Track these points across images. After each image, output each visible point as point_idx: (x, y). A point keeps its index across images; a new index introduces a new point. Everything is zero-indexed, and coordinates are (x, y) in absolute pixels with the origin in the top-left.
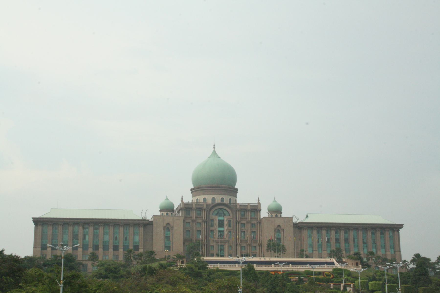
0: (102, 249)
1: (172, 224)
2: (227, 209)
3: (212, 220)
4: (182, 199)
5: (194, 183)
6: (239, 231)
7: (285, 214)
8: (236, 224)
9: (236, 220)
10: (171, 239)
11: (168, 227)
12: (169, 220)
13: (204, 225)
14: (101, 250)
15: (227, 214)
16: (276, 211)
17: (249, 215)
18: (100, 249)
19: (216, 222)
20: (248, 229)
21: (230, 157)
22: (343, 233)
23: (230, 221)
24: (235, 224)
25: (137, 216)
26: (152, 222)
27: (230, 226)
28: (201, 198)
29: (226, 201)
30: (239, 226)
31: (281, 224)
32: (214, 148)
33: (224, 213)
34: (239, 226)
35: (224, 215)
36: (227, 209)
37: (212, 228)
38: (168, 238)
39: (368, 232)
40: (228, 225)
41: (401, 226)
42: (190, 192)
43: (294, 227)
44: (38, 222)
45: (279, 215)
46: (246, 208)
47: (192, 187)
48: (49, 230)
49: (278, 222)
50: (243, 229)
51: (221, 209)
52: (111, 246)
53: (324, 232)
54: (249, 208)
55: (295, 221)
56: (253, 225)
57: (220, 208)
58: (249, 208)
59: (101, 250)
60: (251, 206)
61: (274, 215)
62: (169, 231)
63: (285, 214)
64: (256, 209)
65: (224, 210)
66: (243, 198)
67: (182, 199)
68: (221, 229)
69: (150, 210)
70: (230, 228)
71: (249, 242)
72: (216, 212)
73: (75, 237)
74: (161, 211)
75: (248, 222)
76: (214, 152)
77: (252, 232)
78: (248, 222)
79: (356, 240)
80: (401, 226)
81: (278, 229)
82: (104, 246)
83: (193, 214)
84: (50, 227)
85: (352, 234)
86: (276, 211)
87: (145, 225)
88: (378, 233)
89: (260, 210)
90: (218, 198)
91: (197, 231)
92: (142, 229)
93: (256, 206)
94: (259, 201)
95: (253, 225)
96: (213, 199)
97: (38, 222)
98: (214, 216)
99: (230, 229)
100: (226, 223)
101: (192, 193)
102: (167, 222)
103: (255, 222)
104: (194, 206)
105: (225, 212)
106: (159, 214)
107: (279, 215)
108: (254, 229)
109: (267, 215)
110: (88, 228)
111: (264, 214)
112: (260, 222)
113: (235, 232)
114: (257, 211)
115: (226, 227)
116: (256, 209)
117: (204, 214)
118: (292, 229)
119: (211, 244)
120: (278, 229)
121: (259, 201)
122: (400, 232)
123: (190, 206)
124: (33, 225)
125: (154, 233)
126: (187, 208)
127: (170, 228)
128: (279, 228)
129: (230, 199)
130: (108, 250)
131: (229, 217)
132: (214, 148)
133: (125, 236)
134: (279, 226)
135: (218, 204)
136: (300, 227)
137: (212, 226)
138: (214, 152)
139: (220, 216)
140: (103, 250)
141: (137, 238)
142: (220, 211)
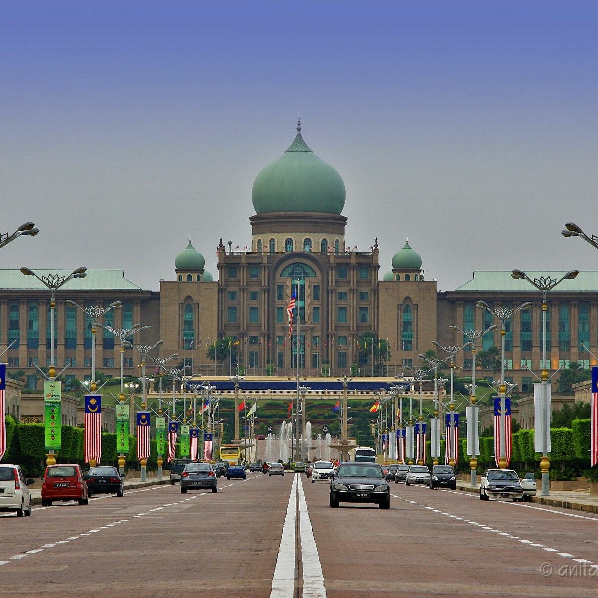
0: (63, 348)
1: (195, 298)
3: (281, 287)
6: (333, 308)
8: (328, 291)
10: (195, 327)
13: (262, 298)
14: (23, 349)
16: (408, 267)
17: (353, 276)
18: (40, 347)
20: (351, 303)
23: (316, 288)
24: (325, 295)
27: (316, 297)
29: (316, 248)
30: (333, 298)
33: (304, 272)
34: (333, 298)
37: (279, 303)
38: (189, 324)
40: (312, 297)
46: (348, 261)
50: (343, 303)
51: (298, 264)
52: (80, 341)
53: (23, 309)
54: (353, 261)
55: (442, 288)
56: (362, 296)
57: (298, 263)
58: (353, 261)
59: (23, 349)
60: (357, 257)
62: (191, 311)
64: (368, 263)
65: (305, 267)
66: (355, 241)
71: (353, 330)
72: (290, 270)
74: (178, 271)
77: (361, 309)
82: (66, 340)
86: (408, 267)
91: (251, 308)
93: (254, 257)
94: (376, 246)
95: (362, 296)
98: (283, 279)
99: (317, 303)
100: (308, 291)
102: (186, 294)
103: (364, 289)
104: (243, 260)
105: (308, 270)
106: (173, 277)
107: (194, 277)
108: (363, 304)
110: (36, 307)
111: (384, 272)
112: (376, 288)
113: (325, 309)
114: (371, 267)
115: (308, 301)
116: (368, 263)
117: (263, 275)
119: (279, 333)
121: (376, 246)
123: (237, 260)
125: (161, 316)
126: (230, 263)
127: (193, 305)
128: (189, 302)
129: (325, 241)
130: (75, 348)
131: (313, 279)
137: (281, 297)
140: (66, 348)
142: (298, 268)
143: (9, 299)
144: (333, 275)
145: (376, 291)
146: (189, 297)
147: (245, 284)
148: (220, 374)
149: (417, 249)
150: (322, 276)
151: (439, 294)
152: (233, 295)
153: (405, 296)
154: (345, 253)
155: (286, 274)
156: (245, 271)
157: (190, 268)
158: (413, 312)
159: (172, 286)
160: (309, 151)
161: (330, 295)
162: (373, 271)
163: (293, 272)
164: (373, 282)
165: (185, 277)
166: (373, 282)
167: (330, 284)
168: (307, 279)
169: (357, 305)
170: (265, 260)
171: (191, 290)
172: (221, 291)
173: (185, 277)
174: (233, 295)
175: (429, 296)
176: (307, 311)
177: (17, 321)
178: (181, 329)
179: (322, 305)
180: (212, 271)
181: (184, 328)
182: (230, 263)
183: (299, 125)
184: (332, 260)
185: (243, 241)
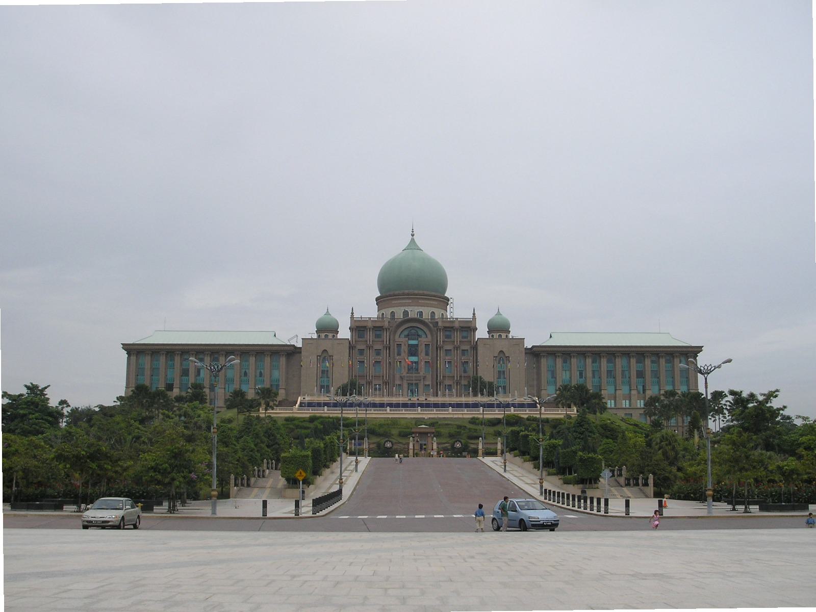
1: (330, 353)
2: (414, 324)
3: (399, 345)
4: (352, 313)
5: (381, 292)
7: (514, 333)
8: (437, 348)
9: (437, 344)
11: (325, 356)
12: (326, 345)
15: (424, 336)
16: (498, 329)
17: (457, 337)
19: (404, 348)
21: (438, 249)
22: (605, 362)
25: (284, 338)
26: (300, 348)
27: (427, 354)
28: (387, 312)
30: (442, 353)
31: (504, 350)
32: (413, 235)
35: (419, 336)
36: (414, 324)
39: (646, 360)
41: (699, 349)
43: (526, 353)
44: (134, 351)
45: (504, 335)
48: (146, 361)
49: (500, 345)
55: (528, 344)
57: (413, 326)
58: (457, 325)
61: (496, 335)
63: (514, 333)
64: (468, 327)
65: (418, 330)
67: (352, 313)
68: (414, 359)
69: (296, 330)
70: (427, 357)
72: (406, 333)
73: (185, 372)
75: (457, 348)
76: (413, 240)
78: (457, 348)
79: (627, 373)
80: (699, 349)
81: (502, 357)
83: (370, 336)
84: (148, 358)
85: (620, 363)
86: (498, 329)
87: (290, 353)
88: (662, 361)
89: (477, 329)
92: (283, 360)
94: (474, 314)
96: (406, 313)
97: (134, 351)
99: (429, 359)
100: (422, 348)
105: (420, 333)
111: (482, 332)
115: (422, 354)
116: (468, 327)
118: (523, 356)
119: (398, 382)
120: (502, 357)
121: (474, 314)
122: (697, 358)
124: (124, 355)
126: (359, 328)
131: (425, 340)
132: (413, 235)
133: (244, 370)
134: (501, 352)
136: (536, 353)
137: (399, 354)
138: (413, 240)
141: (276, 374)
142: (413, 331)
143: (182, 352)
144: (441, 336)
145: (475, 349)
146: (325, 351)
147: (371, 343)
149: (507, 315)
150: (432, 335)
151: (526, 349)
153: (500, 350)
154: (447, 318)
155: (403, 336)
156: (371, 332)
157: (327, 329)
158: (505, 362)
159: (311, 342)
160: (418, 249)
161: (439, 351)
162: (472, 333)
164: (472, 342)
165: (323, 335)
166: (472, 342)
167: (439, 344)
169: (461, 359)
172: (351, 347)
173: (323, 335)
174: (361, 352)
175: (519, 350)
177: (188, 370)
178: (318, 376)
180: (344, 333)
181: (321, 376)
182: (359, 328)
183: (413, 232)
184: (440, 324)
185: (369, 311)
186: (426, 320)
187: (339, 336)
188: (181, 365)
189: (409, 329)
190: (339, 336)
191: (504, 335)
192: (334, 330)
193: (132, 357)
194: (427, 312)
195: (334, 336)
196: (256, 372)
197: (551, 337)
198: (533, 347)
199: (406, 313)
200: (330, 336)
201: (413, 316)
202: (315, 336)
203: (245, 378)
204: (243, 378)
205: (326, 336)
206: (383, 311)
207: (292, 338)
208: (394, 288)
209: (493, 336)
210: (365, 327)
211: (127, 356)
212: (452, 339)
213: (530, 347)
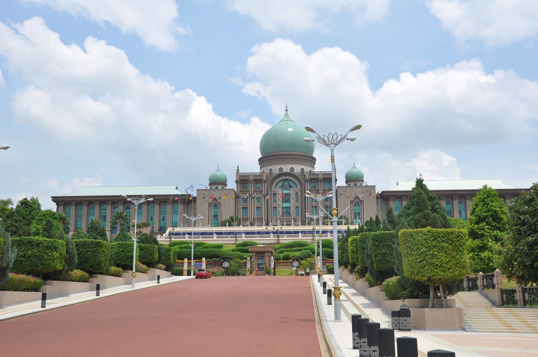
4: (238, 170)
15: (294, 186)
19: (279, 196)
27: (297, 201)
28: (267, 169)
33: (290, 186)
37: (274, 205)
40: (295, 199)
42: (258, 163)
45: (358, 184)
46: (317, 177)
47: (260, 156)
51: (286, 180)
54: (321, 177)
58: (321, 177)
61: (352, 184)
66: (322, 166)
67: (238, 170)
68: (286, 205)
72: (280, 184)
74: (210, 185)
83: (251, 187)
86: (354, 179)
90: (286, 168)
98: (276, 190)
100: (293, 196)
101: (260, 164)
105: (292, 184)
109: (345, 185)
115: (293, 202)
123: (247, 178)
126: (243, 180)
131: (296, 189)
135: (286, 174)
137: (275, 201)
139: (286, 189)
142: (286, 183)
148: (194, 255)
152: (245, 200)
157: (217, 183)
163: (282, 186)
168: (291, 189)
170: (265, 178)
171: (216, 195)
172: (237, 197)
174: (245, 200)
176: (293, 209)
179: (301, 204)
180: (232, 185)
184: (307, 177)
186: (296, 174)
187: (227, 187)
188: (100, 212)
189: (282, 182)
190: (227, 187)
191: (358, 184)
192: (224, 183)
193: (60, 207)
194: (297, 168)
195: (223, 188)
196: (159, 217)
197: (398, 184)
198: (383, 192)
199: (281, 169)
200: (220, 187)
201: (286, 171)
202: (209, 188)
203: (151, 222)
204: (161, 222)
205: (217, 187)
206: (263, 169)
207: (188, 188)
208: (273, 151)
209: (349, 185)
210: (248, 180)
211: (56, 206)
212: (317, 188)
213: (380, 192)
